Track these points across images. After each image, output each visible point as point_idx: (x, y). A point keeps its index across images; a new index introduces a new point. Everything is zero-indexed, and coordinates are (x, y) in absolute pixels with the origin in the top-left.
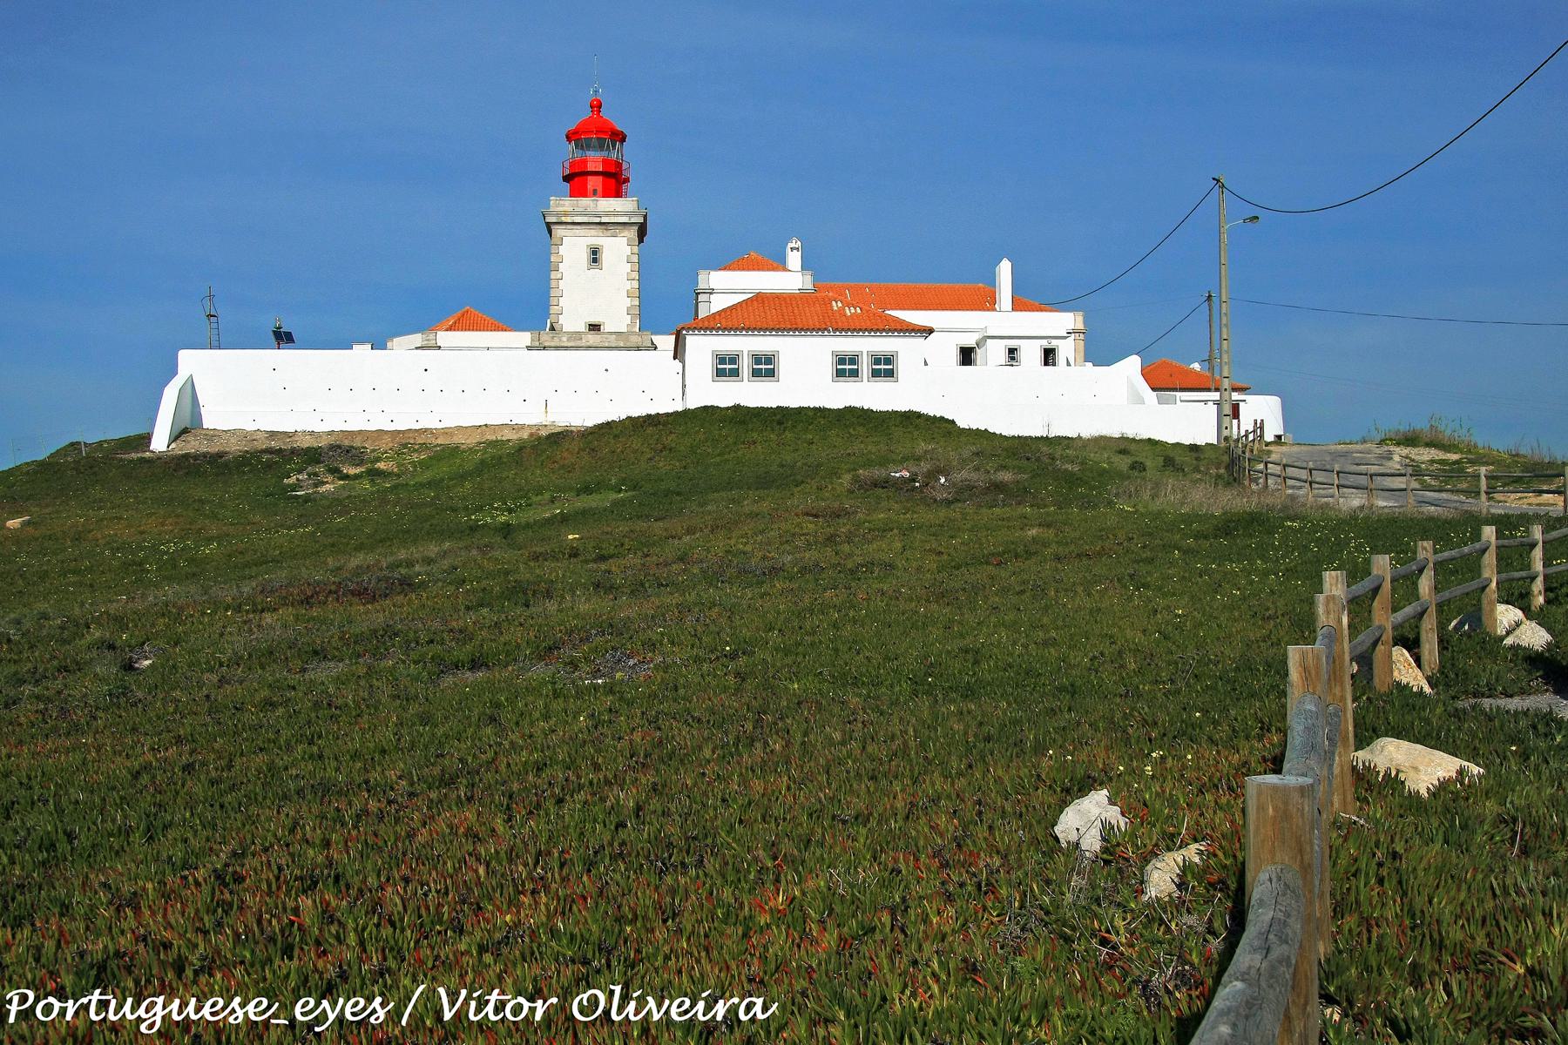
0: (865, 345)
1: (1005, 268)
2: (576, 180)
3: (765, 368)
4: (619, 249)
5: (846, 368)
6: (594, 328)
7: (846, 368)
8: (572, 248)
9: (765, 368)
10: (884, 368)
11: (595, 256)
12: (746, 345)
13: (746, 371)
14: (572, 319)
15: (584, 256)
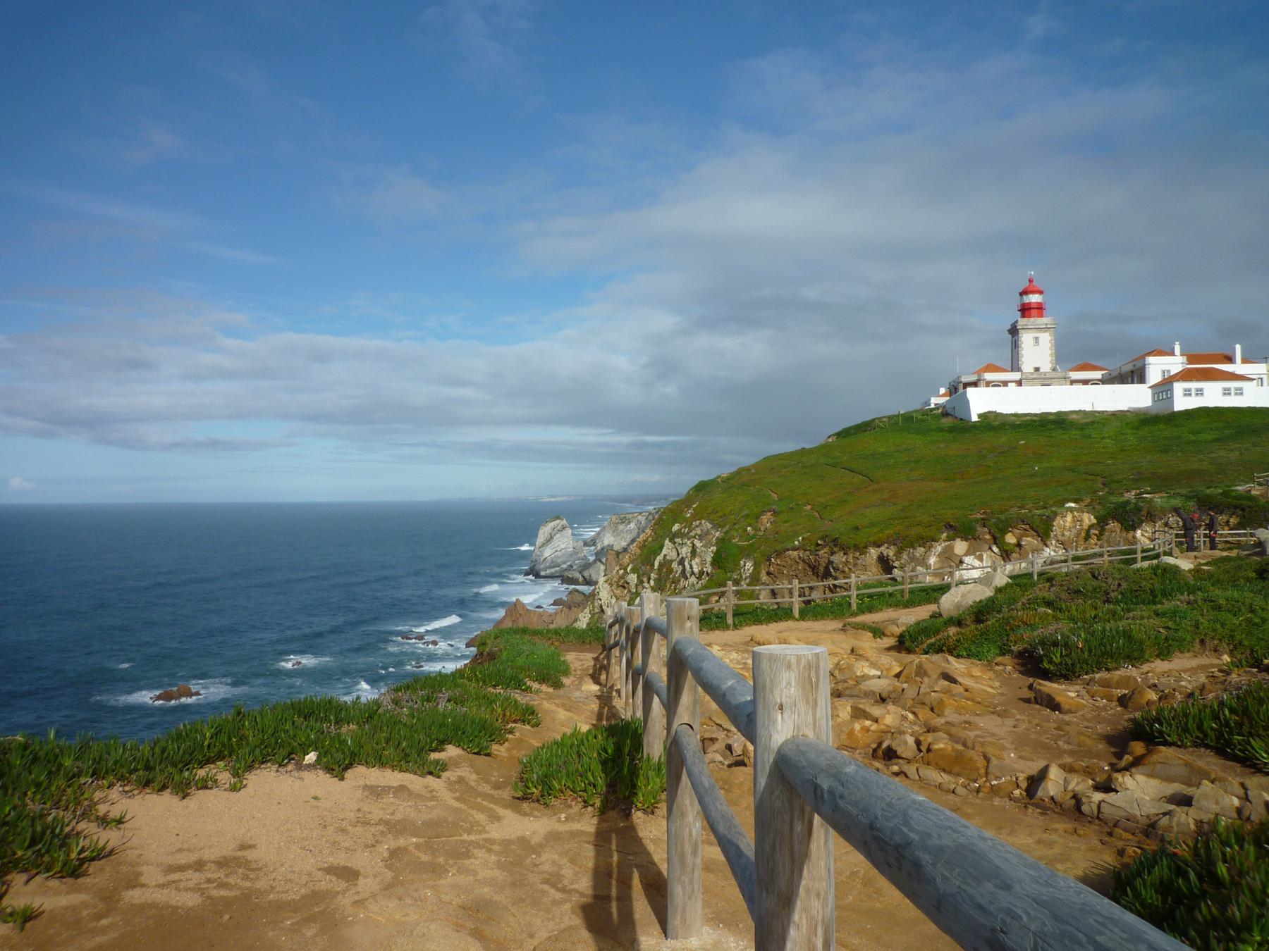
0: (1232, 385)
1: (1238, 348)
2: (1025, 310)
3: (1200, 392)
4: (1046, 339)
5: (1227, 392)
6: (1037, 369)
7: (1227, 392)
8: (1026, 339)
9: (1200, 392)
10: (1239, 392)
11: (1037, 338)
12: (1193, 385)
13: (1193, 393)
14: (1027, 366)
15: (1032, 341)
